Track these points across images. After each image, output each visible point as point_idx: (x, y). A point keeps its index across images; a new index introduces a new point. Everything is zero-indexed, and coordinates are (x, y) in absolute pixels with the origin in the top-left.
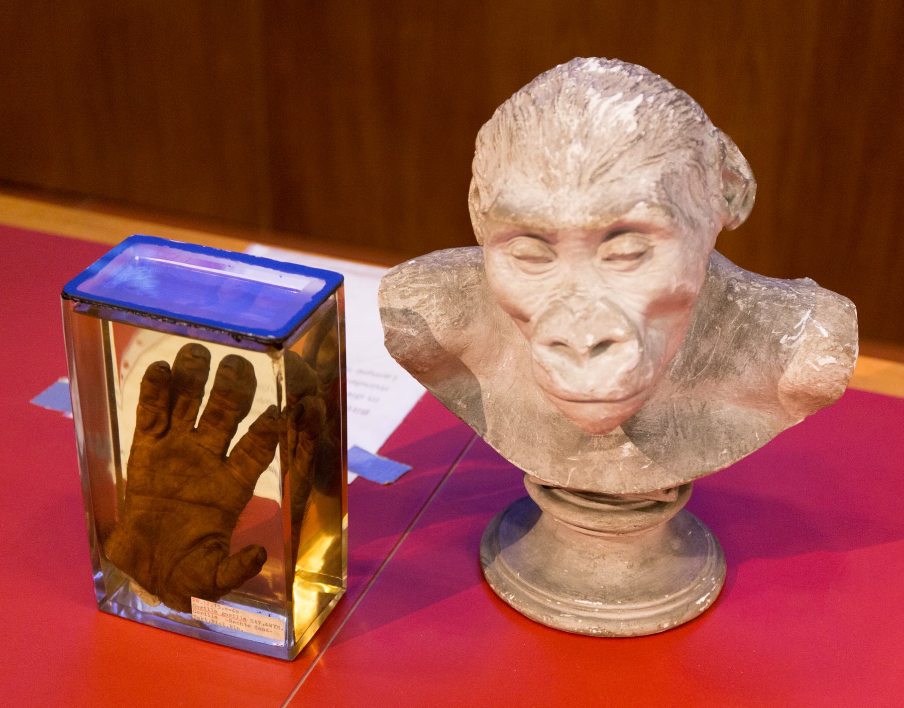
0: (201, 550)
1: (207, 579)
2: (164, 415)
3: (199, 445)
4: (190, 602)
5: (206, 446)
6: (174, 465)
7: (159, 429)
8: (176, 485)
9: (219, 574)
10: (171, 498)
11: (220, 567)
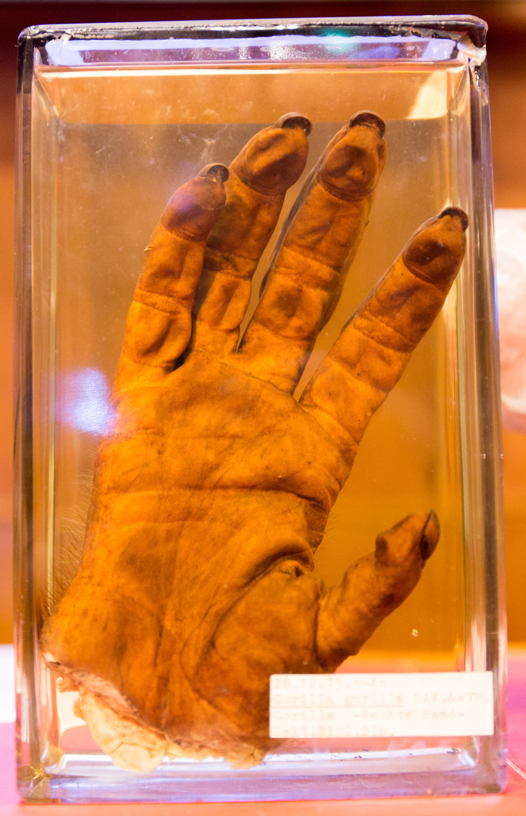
0: (275, 577)
1: (301, 629)
2: (185, 317)
3: (250, 374)
4: (264, 697)
5: (262, 377)
6: (204, 417)
7: (172, 349)
8: (210, 456)
9: (323, 617)
10: (197, 486)
11: (323, 602)
